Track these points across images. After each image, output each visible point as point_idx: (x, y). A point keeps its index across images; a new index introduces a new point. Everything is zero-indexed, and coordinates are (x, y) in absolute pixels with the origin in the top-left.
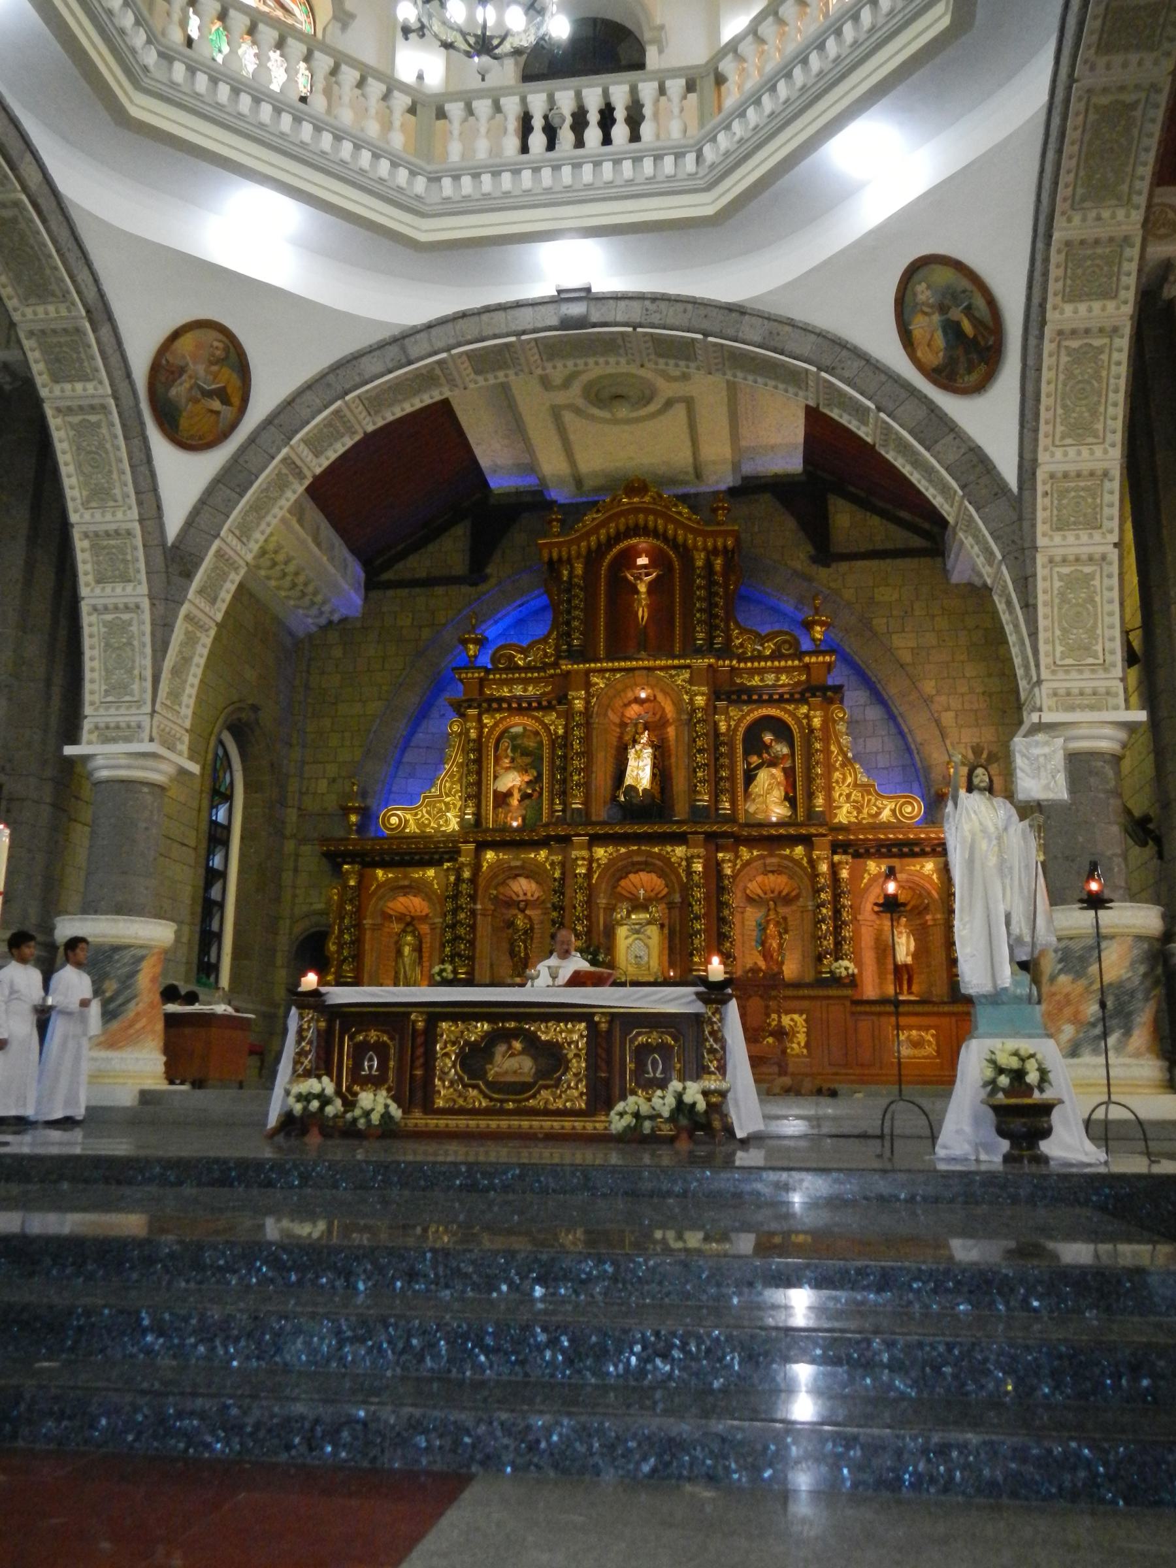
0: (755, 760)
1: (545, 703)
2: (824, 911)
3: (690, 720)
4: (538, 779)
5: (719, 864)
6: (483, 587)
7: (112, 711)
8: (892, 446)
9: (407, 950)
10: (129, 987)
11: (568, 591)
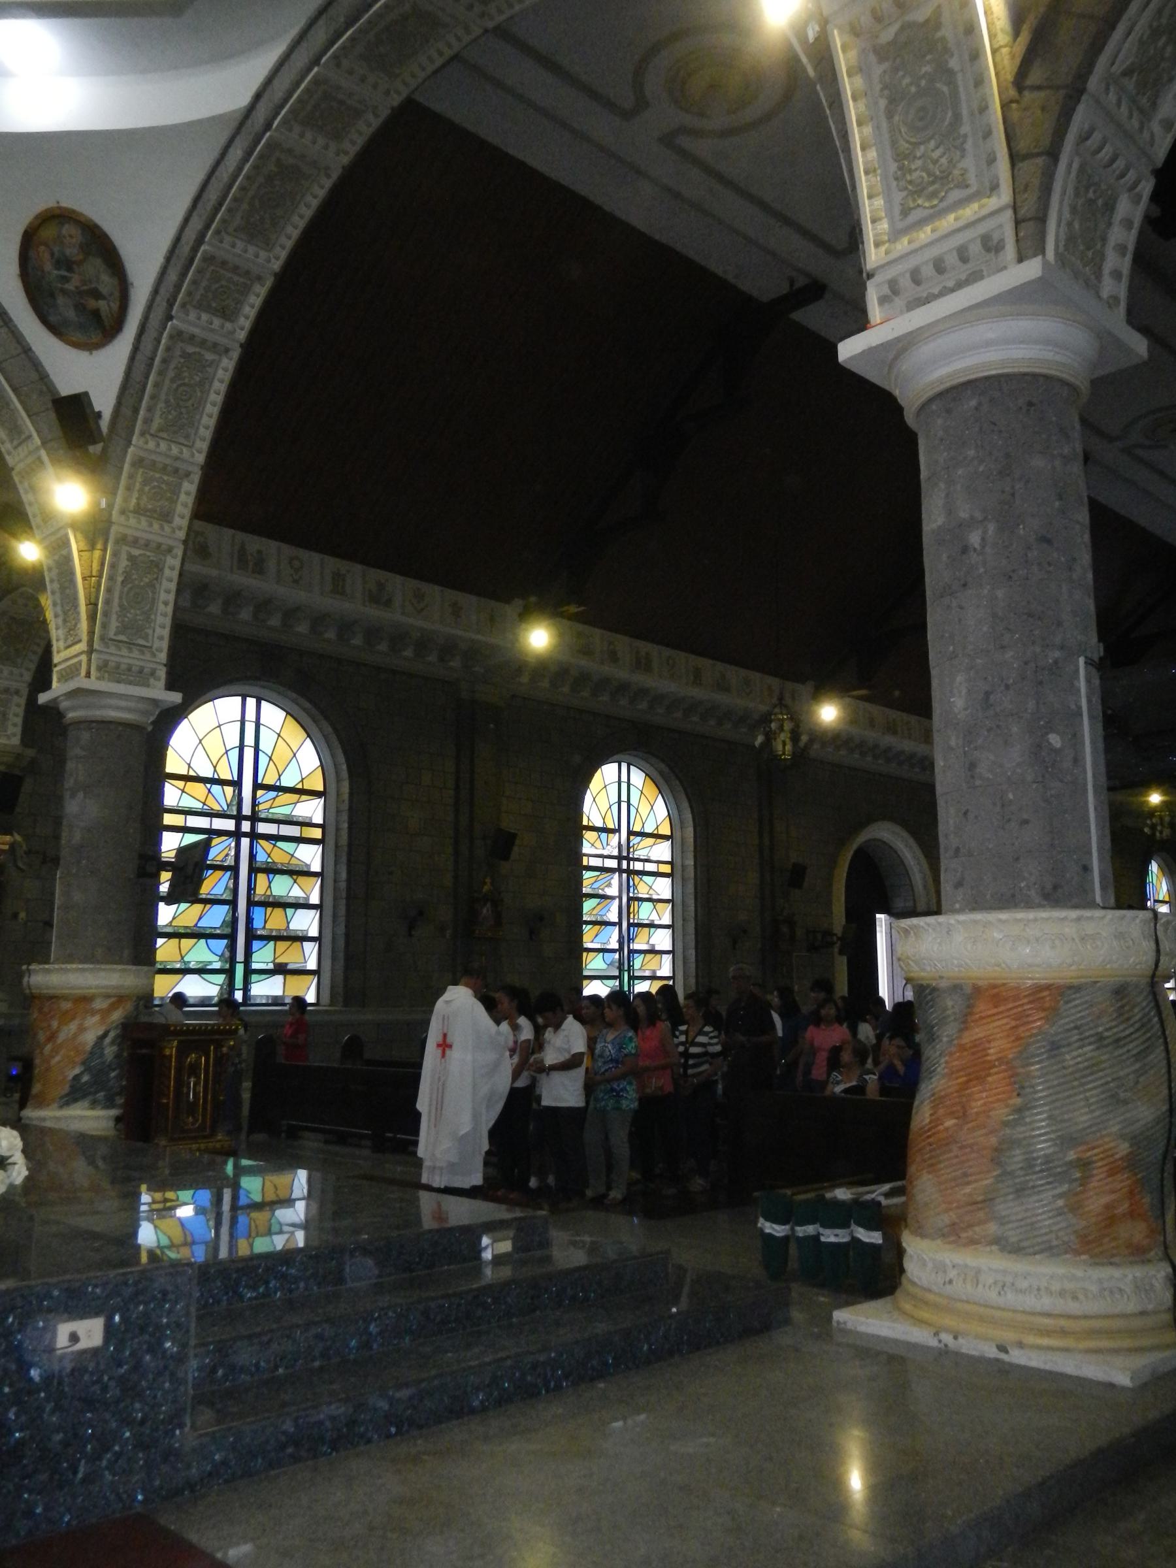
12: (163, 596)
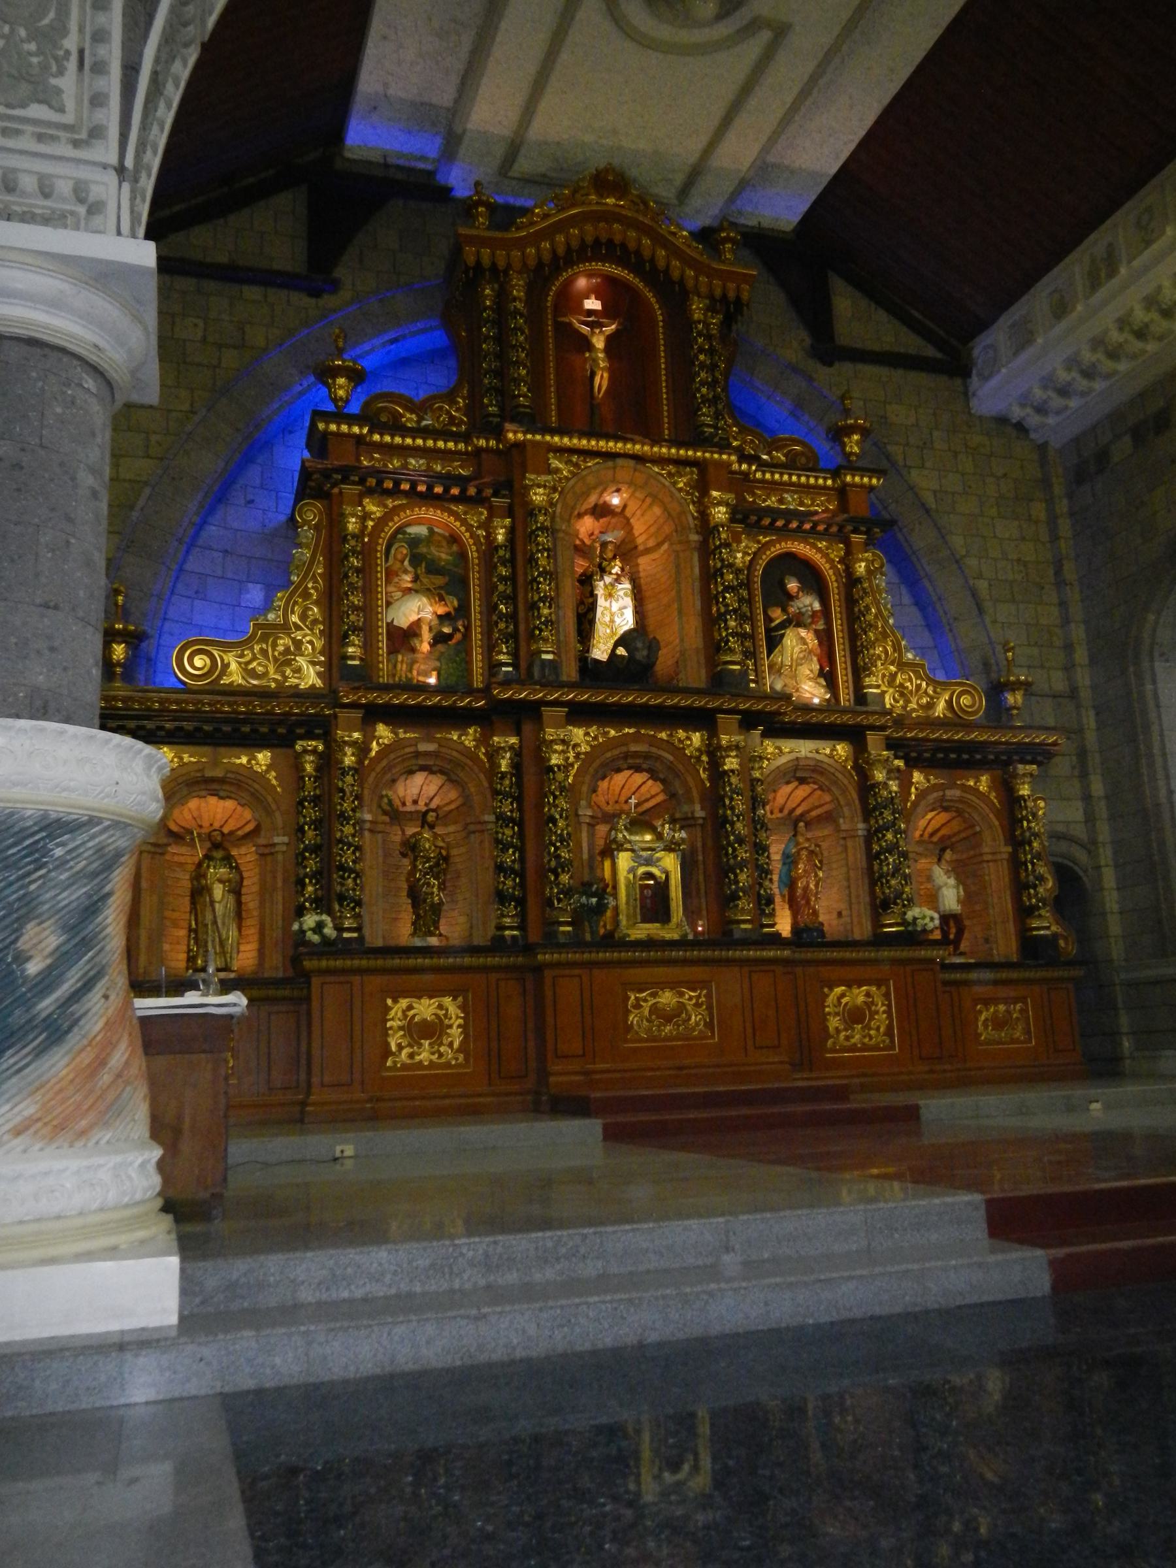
0: (778, 615)
1: (472, 491)
4: (463, 610)
6: (329, 301)
9: (218, 891)
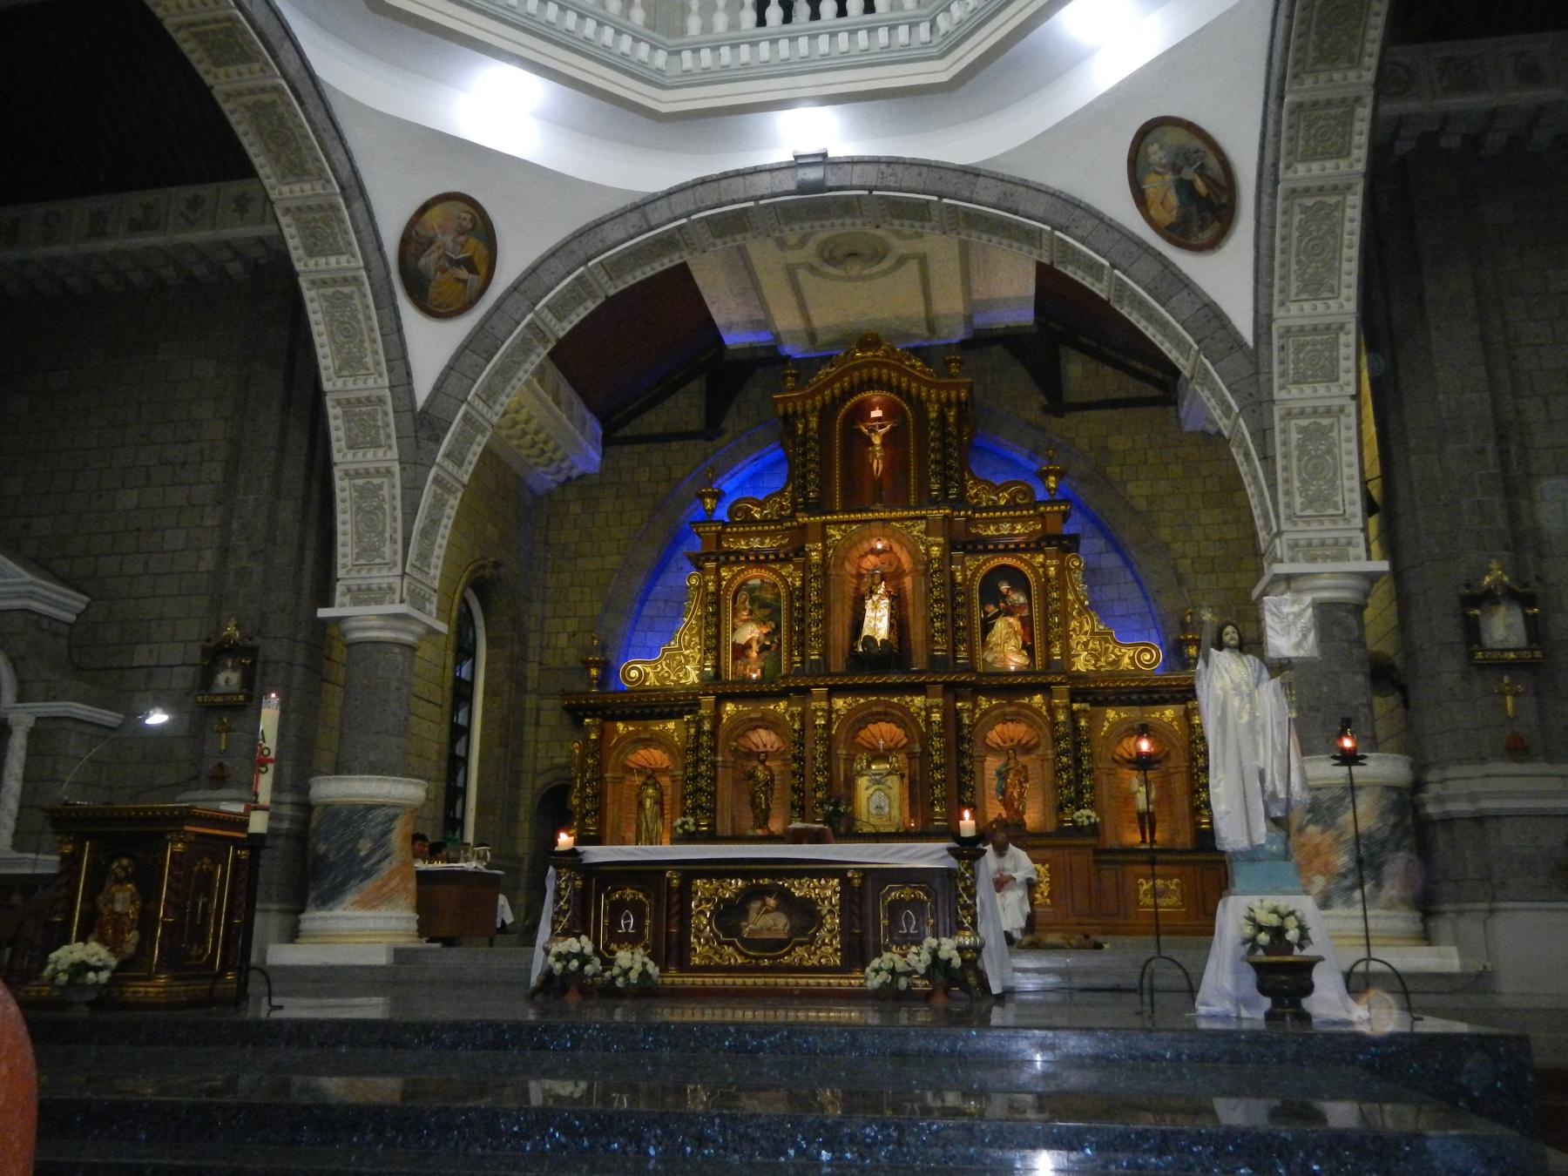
0: (992, 609)
1: (782, 556)
2: (1064, 759)
3: (927, 570)
4: (777, 630)
5: (958, 713)
6: (718, 442)
7: (364, 573)
8: (1127, 302)
9: (648, 803)
10: (382, 846)
11: (804, 444)
12: (1345, 459)
